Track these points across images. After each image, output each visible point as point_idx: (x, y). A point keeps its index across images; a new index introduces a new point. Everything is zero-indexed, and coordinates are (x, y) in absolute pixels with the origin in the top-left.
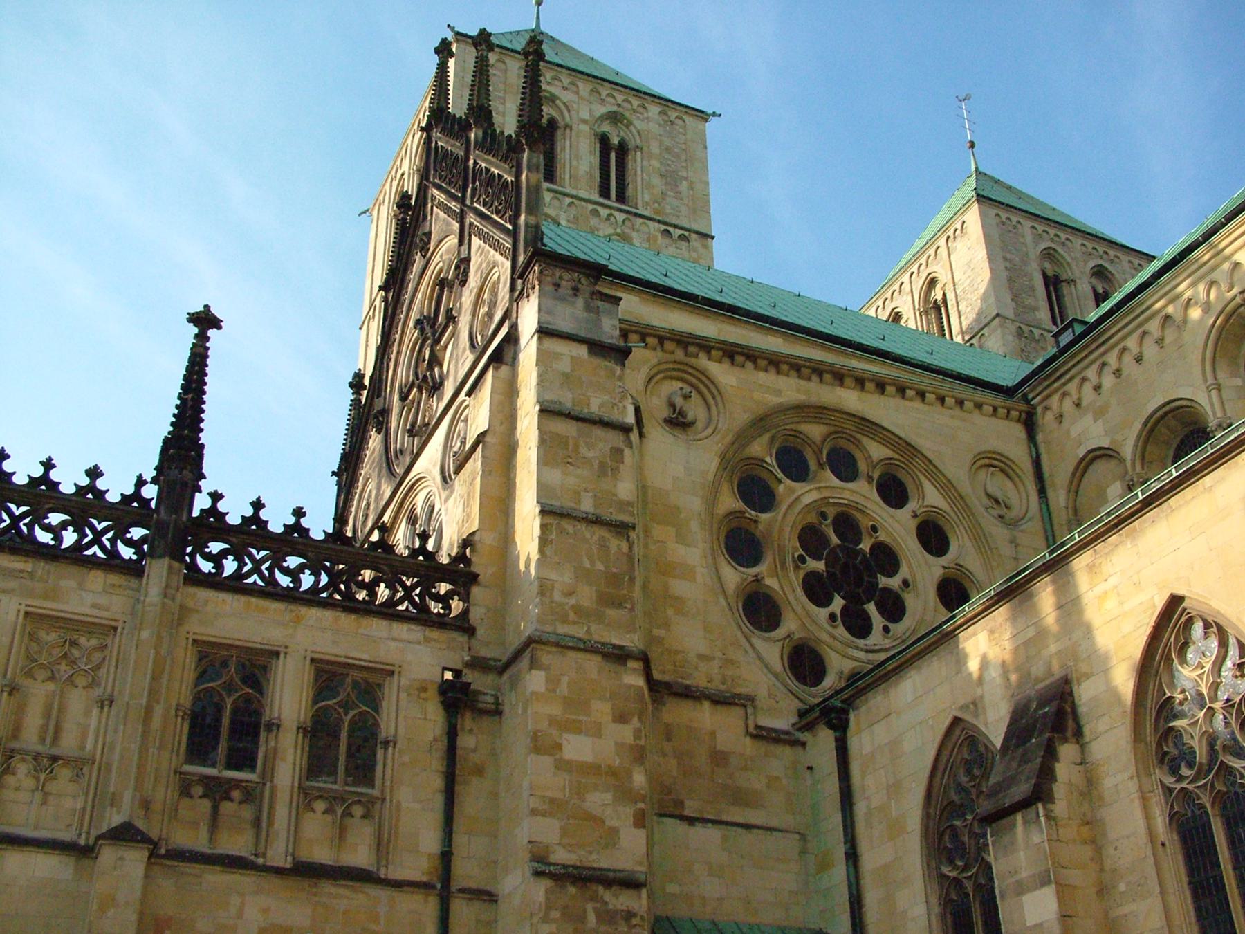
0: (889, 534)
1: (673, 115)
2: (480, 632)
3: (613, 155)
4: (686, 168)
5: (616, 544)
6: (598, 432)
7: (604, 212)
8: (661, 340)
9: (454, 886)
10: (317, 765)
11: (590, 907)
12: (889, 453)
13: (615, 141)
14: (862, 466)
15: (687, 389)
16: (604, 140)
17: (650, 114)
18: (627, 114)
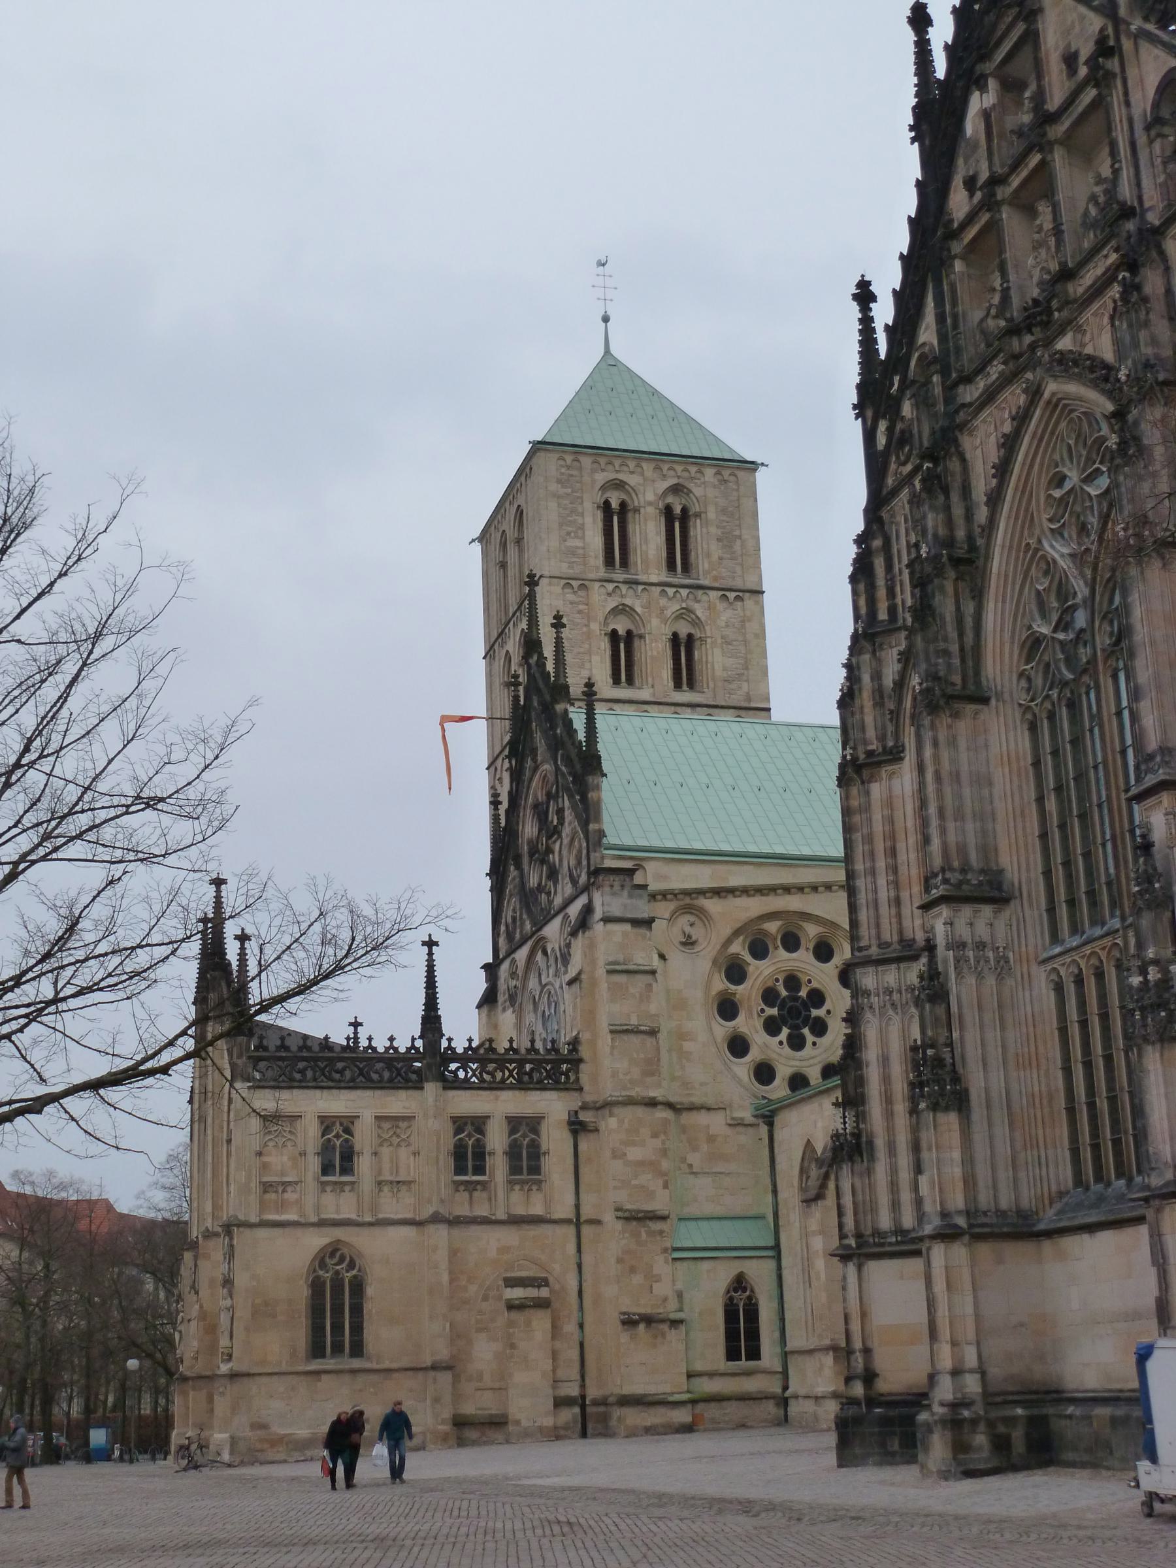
0: (819, 982)
1: (726, 473)
2: (586, 1088)
3: (677, 525)
4: (740, 526)
5: (650, 1041)
6: (639, 977)
7: (671, 591)
8: (675, 895)
9: (583, 1219)
10: (515, 1169)
11: (643, 1230)
12: (821, 929)
13: (678, 510)
14: (803, 942)
15: (692, 919)
16: (668, 511)
17: (707, 479)
18: (686, 484)
